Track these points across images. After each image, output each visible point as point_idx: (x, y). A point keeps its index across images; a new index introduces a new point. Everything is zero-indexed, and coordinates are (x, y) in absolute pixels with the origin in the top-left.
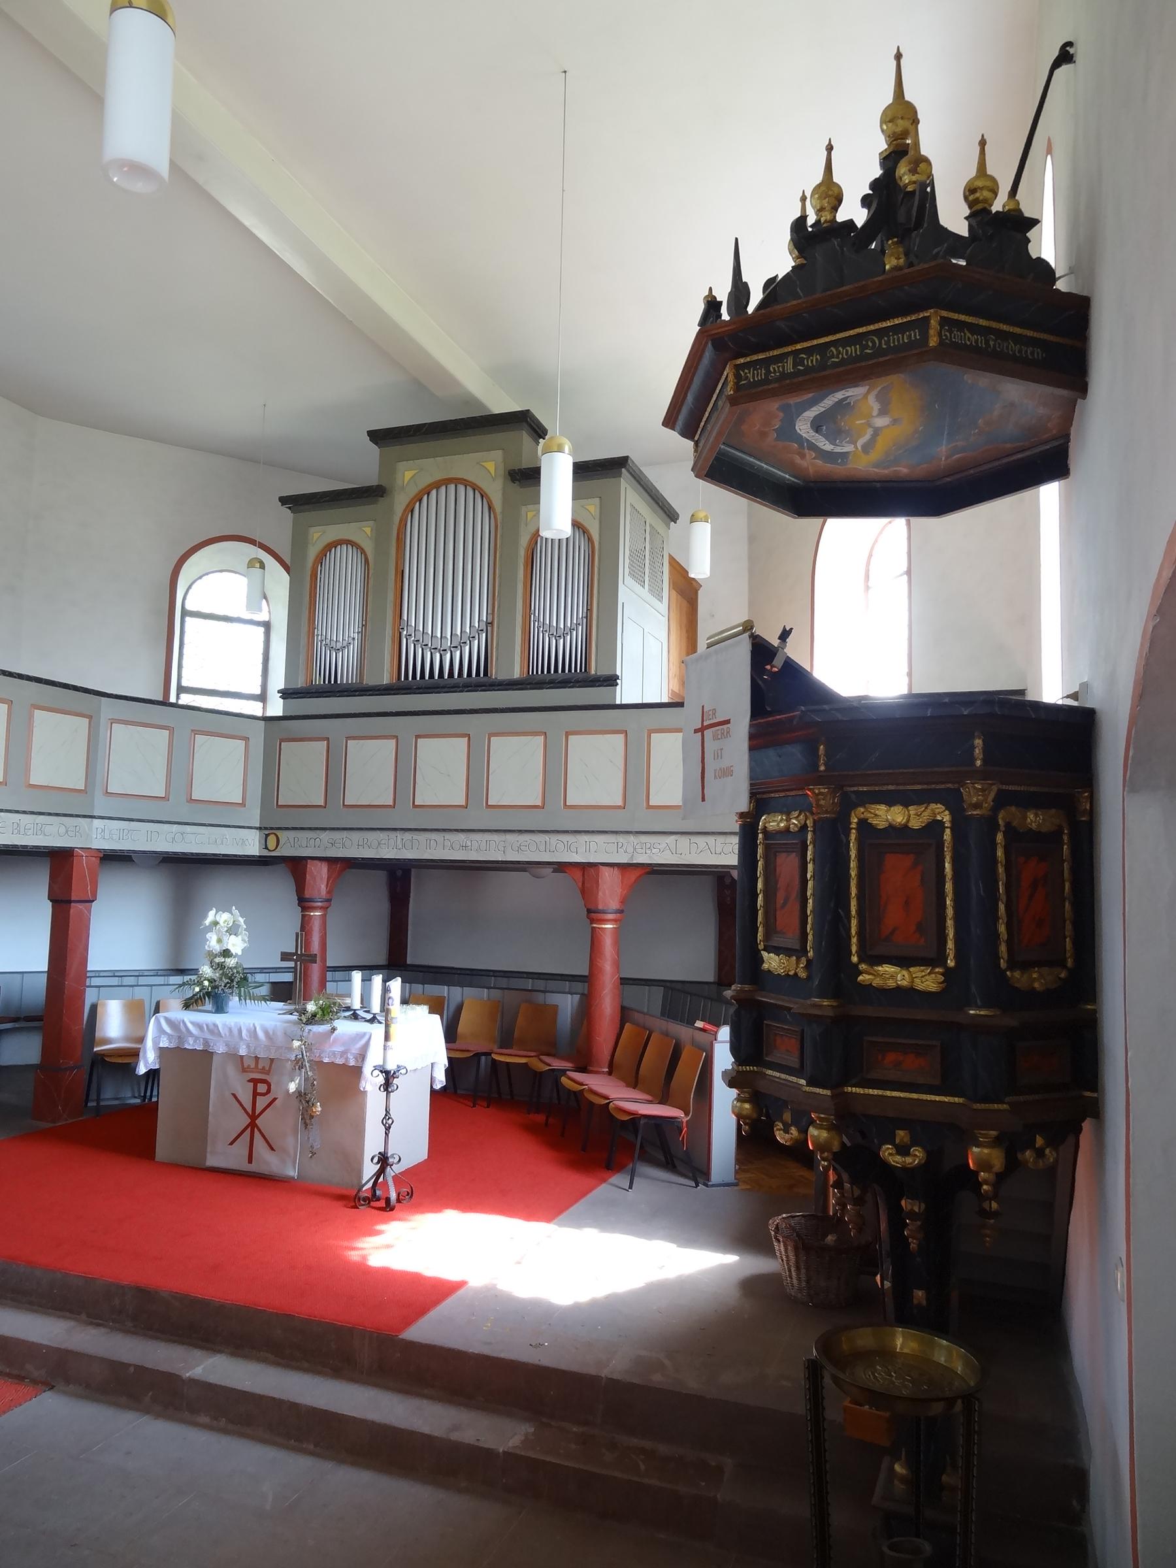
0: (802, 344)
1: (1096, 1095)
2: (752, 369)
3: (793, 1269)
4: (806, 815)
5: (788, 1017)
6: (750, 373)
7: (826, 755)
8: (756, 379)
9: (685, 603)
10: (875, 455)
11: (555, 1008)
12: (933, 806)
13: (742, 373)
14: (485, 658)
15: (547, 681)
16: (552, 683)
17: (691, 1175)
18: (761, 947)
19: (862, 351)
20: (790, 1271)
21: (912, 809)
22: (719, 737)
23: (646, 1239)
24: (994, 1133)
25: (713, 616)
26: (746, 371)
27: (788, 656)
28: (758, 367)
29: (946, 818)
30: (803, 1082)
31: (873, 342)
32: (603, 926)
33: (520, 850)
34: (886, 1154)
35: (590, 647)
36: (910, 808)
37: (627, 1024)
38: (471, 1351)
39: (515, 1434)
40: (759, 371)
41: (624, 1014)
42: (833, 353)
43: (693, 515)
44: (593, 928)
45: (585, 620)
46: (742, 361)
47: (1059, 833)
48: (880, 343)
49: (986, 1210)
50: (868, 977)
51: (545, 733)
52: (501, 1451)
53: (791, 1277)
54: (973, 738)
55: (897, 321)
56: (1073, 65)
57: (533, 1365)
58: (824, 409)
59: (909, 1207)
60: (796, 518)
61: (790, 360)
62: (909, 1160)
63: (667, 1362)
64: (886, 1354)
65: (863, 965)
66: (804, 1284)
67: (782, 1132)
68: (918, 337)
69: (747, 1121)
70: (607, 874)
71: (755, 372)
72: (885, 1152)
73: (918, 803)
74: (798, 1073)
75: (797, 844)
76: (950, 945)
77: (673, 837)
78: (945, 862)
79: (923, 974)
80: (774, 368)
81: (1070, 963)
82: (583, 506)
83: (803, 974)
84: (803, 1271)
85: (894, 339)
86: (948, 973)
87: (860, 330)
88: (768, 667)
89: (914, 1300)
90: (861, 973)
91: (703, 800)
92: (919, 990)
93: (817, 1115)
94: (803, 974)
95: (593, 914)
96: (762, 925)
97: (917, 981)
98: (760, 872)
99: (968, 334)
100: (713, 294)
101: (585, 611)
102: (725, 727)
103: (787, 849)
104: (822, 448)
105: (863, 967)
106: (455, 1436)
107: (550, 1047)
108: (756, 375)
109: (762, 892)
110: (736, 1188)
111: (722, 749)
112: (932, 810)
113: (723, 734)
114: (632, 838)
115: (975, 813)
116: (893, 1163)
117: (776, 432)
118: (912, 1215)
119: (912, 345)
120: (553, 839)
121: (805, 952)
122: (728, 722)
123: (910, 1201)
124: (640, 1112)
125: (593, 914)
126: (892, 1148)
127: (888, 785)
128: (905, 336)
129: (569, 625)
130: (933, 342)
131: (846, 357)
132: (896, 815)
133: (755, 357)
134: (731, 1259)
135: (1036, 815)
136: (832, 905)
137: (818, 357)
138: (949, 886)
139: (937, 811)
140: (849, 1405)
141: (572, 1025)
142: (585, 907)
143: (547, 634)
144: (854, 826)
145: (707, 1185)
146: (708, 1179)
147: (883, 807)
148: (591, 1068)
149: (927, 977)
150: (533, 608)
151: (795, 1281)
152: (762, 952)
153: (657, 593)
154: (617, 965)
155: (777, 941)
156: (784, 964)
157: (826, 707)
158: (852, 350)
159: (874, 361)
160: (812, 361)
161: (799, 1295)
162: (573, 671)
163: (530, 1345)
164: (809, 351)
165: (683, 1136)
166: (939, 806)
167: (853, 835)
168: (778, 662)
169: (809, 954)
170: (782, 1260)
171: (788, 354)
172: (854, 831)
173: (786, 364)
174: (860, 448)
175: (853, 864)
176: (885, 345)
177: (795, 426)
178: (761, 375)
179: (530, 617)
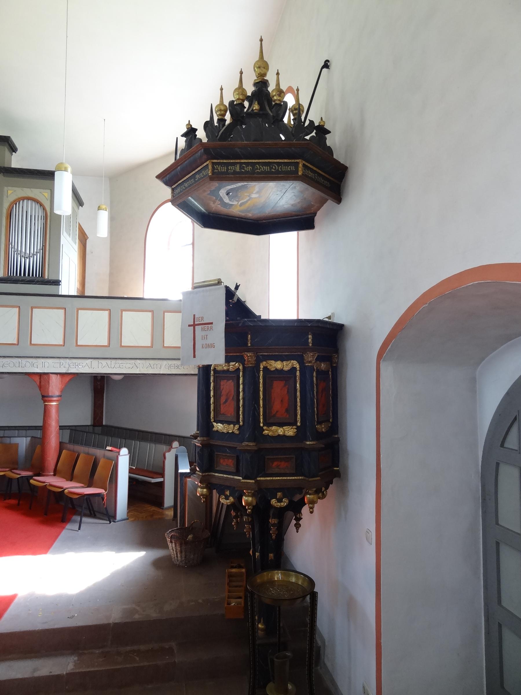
0: (244, 160)
1: (338, 469)
2: (220, 166)
3: (178, 553)
4: (239, 364)
5: (228, 450)
6: (219, 167)
7: (251, 339)
8: (222, 171)
9: (82, 245)
10: (242, 208)
11: (17, 445)
12: (292, 361)
13: (215, 166)
14: (19, 273)
15: (20, 280)
16: (23, 281)
17: (108, 519)
18: (212, 420)
19: (270, 170)
20: (177, 554)
21: (285, 363)
22: (206, 329)
23: (94, 552)
24: (315, 489)
25: (92, 253)
26: (217, 166)
27: (238, 297)
28: (223, 165)
29: (298, 366)
30: (241, 478)
31: (275, 167)
32: (50, 404)
33: (3, 366)
34: (274, 503)
35: (45, 266)
36: (284, 362)
37: (64, 451)
38: (38, 629)
39: (69, 663)
40: (224, 167)
41: (61, 446)
42: (257, 167)
43: (99, 207)
44: (45, 405)
45: (41, 251)
46: (216, 161)
47: (328, 371)
48: (278, 168)
49: (298, 517)
50: (266, 432)
51: (19, 307)
52: (65, 673)
53: (177, 557)
54: (308, 335)
55: (286, 161)
56: (328, 69)
57: (73, 627)
58: (236, 187)
59: (273, 522)
60: (203, 228)
61: (238, 166)
62: (282, 504)
63: (138, 608)
64: (272, 582)
65: (265, 427)
66: (183, 559)
67: (224, 499)
68: (294, 170)
69: (204, 497)
70: (54, 378)
71: (222, 167)
72: (273, 502)
73: (287, 360)
74: (237, 473)
75: (235, 376)
76: (299, 417)
77: (90, 360)
78: (297, 384)
79: (289, 429)
80: (231, 168)
81: (331, 421)
82: (40, 192)
83: (237, 432)
84: (183, 553)
85: (284, 168)
86: (298, 428)
87: (270, 161)
88: (231, 301)
89: (269, 558)
90: (264, 430)
91: (194, 357)
92: (286, 436)
93: (246, 491)
94: (237, 432)
95: (46, 398)
96: (213, 411)
97: (286, 432)
98: (212, 388)
99: (310, 172)
100: (191, 124)
101: (42, 246)
102: (210, 326)
103: (228, 379)
104: (224, 201)
105: (265, 428)
106: (37, 674)
107: (14, 465)
108: (222, 169)
109: (213, 397)
110: (128, 521)
112: (292, 363)
113: (208, 328)
114: (68, 360)
115: (309, 364)
116: (276, 506)
117: (210, 192)
118: (274, 525)
119: (291, 172)
120: (24, 361)
121: (238, 422)
122: (212, 323)
123: (273, 519)
124: (85, 493)
125: (45, 398)
126: (276, 500)
127: (276, 352)
128: (289, 168)
129: (32, 252)
130: (300, 173)
131: (263, 170)
132: (278, 365)
133: (222, 161)
134: (141, 554)
135: (324, 365)
136: (254, 403)
137: (251, 167)
138: (298, 394)
139: (294, 363)
140: (227, 606)
141: (26, 452)
142: (41, 394)
143: (19, 256)
144: (261, 369)
145: (115, 522)
146: (115, 519)
147: (273, 362)
148: (44, 474)
149: (290, 430)
150: (11, 241)
151: (179, 558)
152: (213, 423)
153: (74, 240)
154: (58, 421)
155: (221, 418)
156: (226, 428)
157: (256, 320)
158: (266, 168)
159: (276, 175)
160: (248, 168)
161: (181, 564)
162: (34, 276)
163: (68, 618)
164: (247, 164)
165: (105, 502)
166: (295, 361)
167: (261, 373)
168: (235, 299)
169: (241, 423)
170: (173, 550)
171: (237, 163)
172: (261, 372)
173: (236, 167)
174: (239, 204)
175: (261, 385)
176: (280, 169)
177: (220, 191)
178: (224, 170)
179: (9, 245)
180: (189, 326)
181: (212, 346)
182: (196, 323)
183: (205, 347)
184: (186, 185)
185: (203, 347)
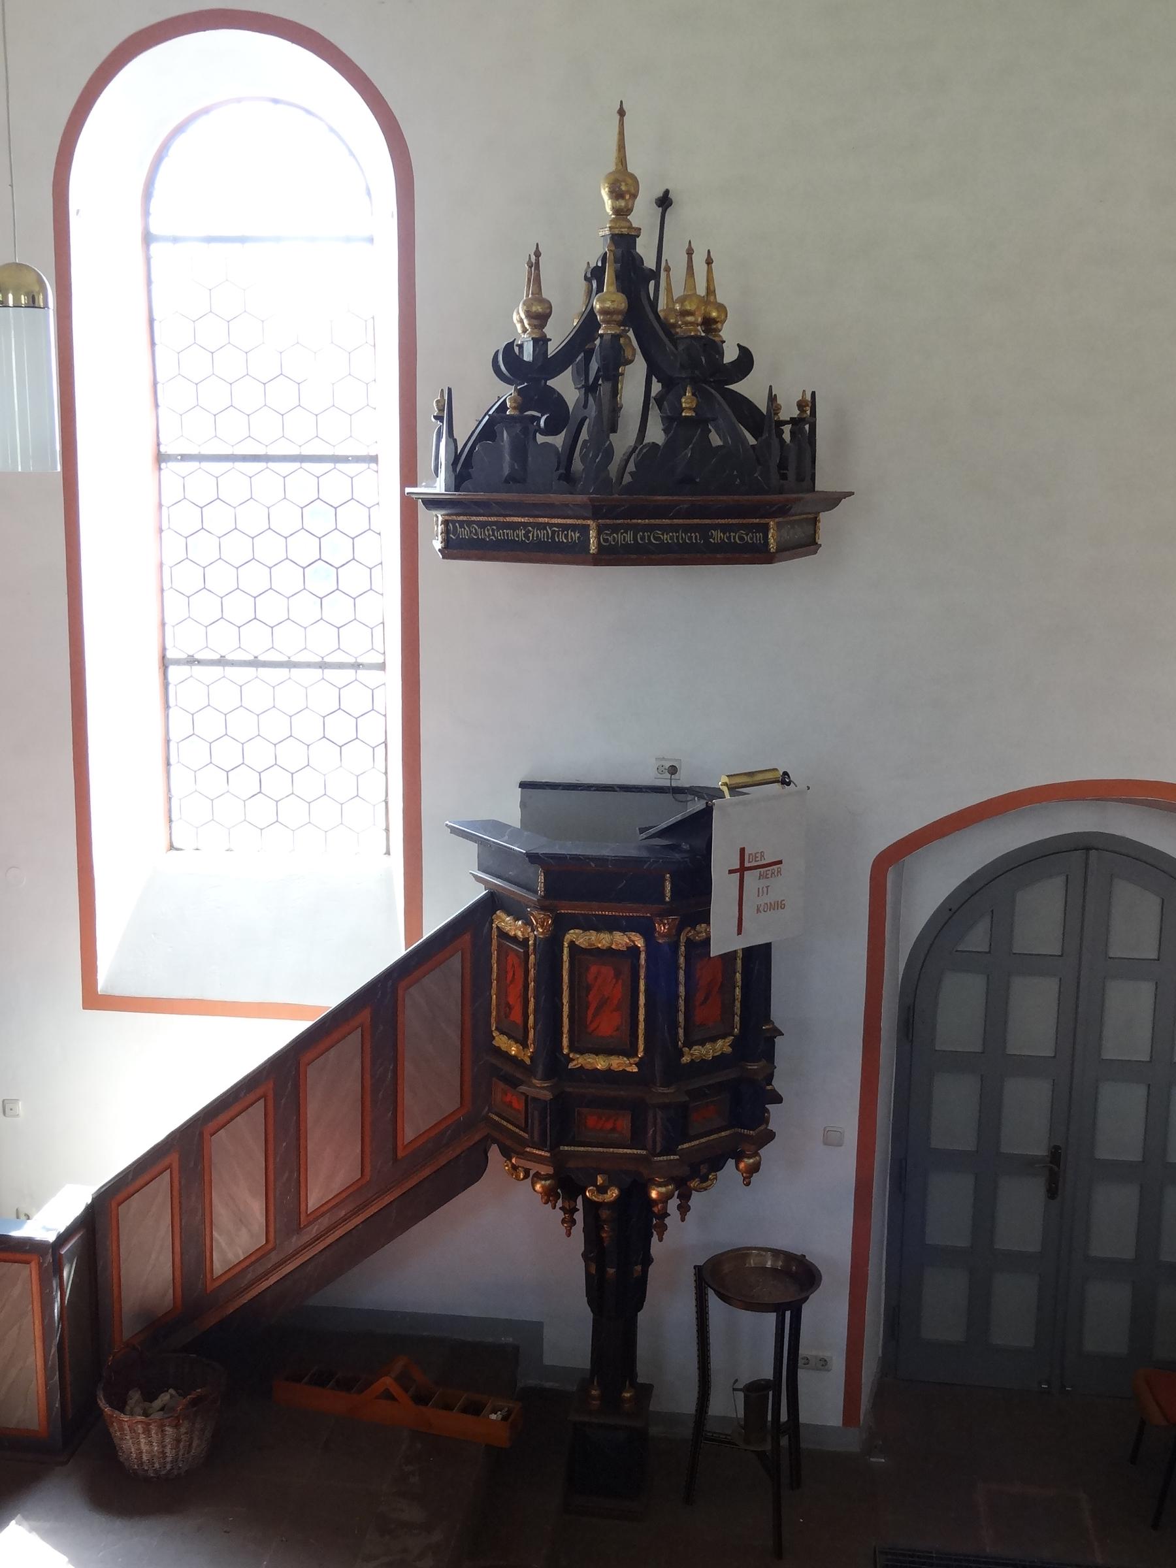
22: (769, 876)
102: (775, 867)
111: (767, 887)
122: (780, 862)
180: (731, 872)
181: (780, 905)
182: (747, 865)
183: (764, 909)
184: (666, 538)
185: (758, 911)
